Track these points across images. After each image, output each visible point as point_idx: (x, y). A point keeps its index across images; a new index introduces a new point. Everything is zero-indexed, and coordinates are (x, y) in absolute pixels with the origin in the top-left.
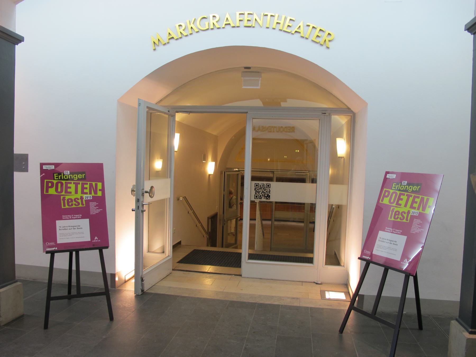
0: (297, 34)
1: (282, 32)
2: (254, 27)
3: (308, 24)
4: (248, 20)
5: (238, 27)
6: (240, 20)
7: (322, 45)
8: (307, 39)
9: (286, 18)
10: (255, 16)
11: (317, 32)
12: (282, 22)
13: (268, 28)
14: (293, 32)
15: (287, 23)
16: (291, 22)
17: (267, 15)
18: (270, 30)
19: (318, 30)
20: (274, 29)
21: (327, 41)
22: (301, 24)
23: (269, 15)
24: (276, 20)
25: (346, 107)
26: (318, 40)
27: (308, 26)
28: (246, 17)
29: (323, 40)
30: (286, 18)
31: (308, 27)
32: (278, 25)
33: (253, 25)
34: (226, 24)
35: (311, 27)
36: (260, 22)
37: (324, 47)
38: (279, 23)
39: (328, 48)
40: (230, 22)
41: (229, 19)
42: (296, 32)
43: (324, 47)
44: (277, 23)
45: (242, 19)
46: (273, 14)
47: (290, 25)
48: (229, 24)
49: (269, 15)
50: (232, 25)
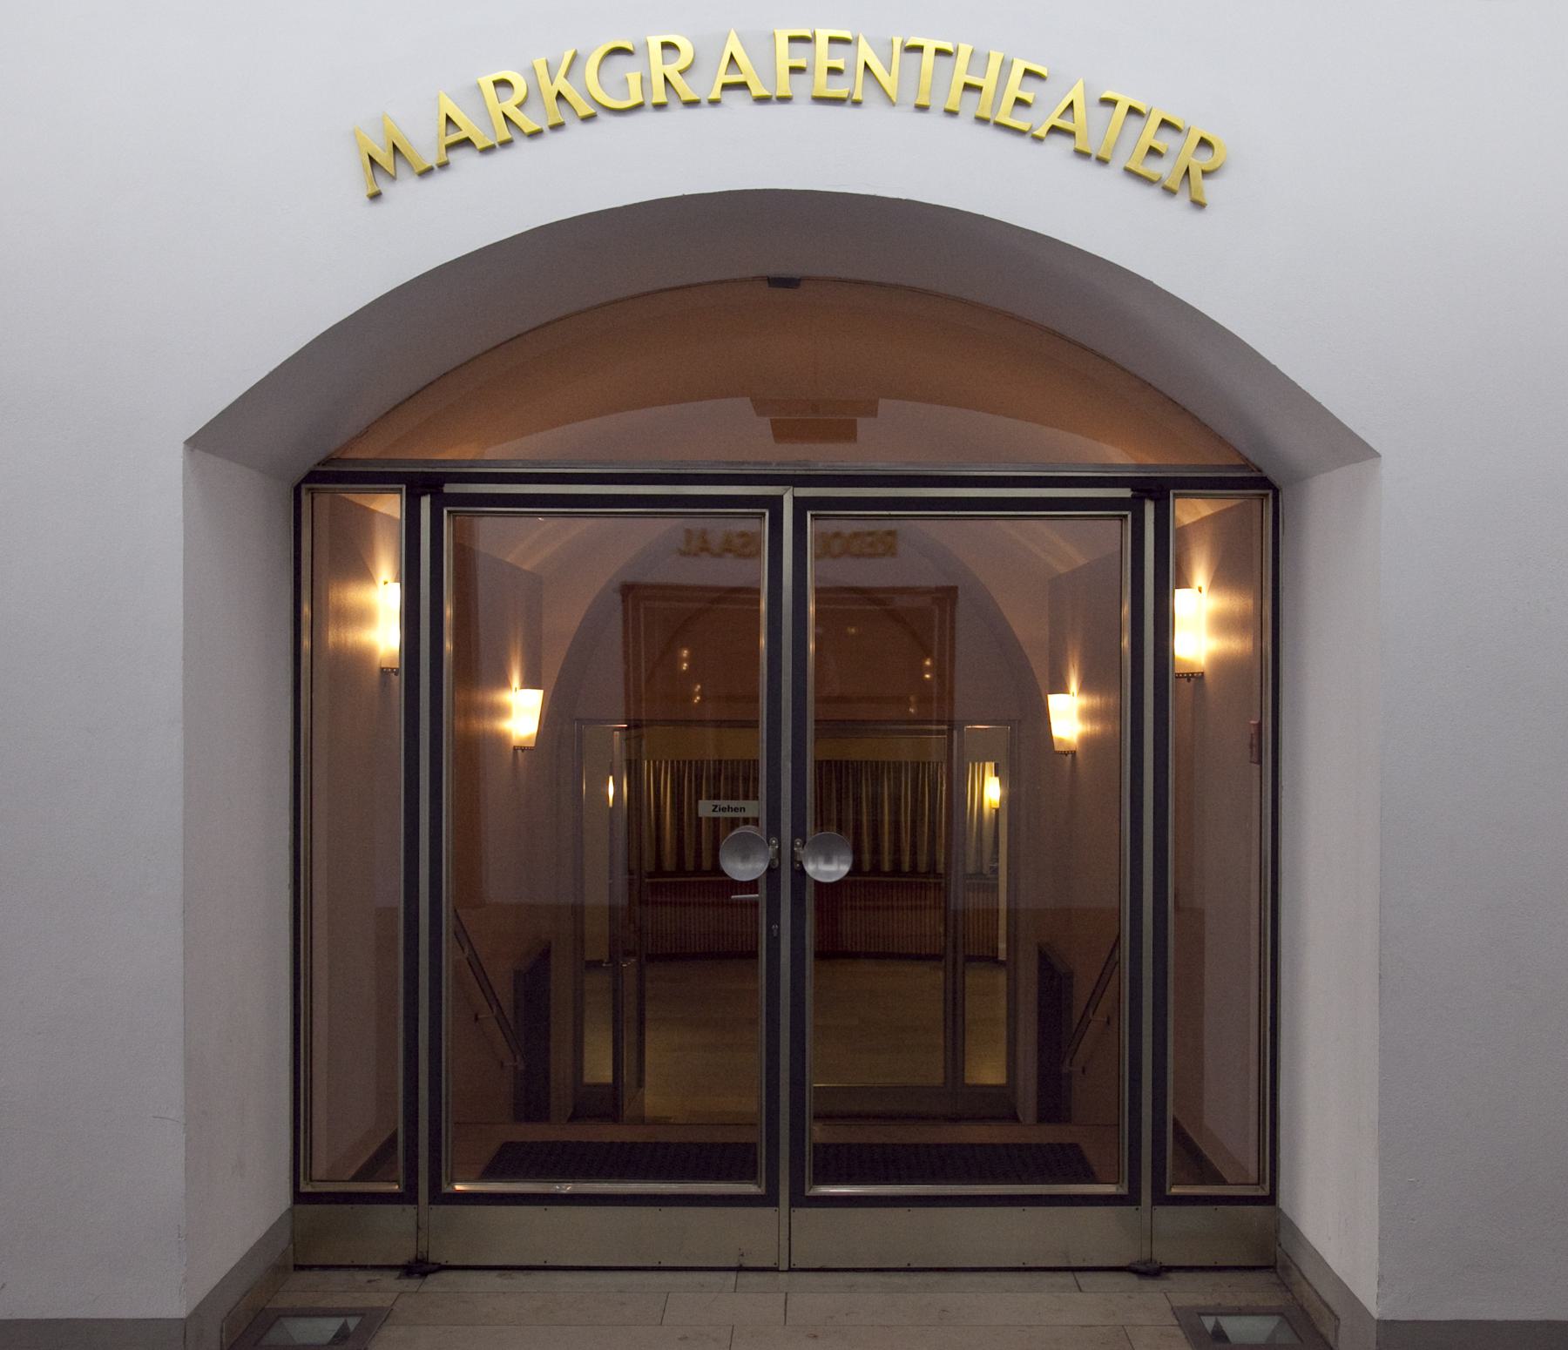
0: (1058, 140)
1: (988, 132)
2: (857, 103)
3: (1108, 95)
4: (832, 71)
5: (784, 100)
6: (794, 70)
7: (1170, 192)
8: (1102, 161)
9: (1006, 66)
10: (865, 53)
11: (1149, 133)
12: (988, 83)
13: (922, 108)
14: (1042, 131)
15: (1014, 88)
16: (1031, 81)
17: (920, 49)
18: (934, 120)
19: (1154, 122)
20: (952, 113)
21: (1195, 173)
22: (1076, 94)
23: (930, 46)
24: (961, 76)
25: (1238, 461)
26: (1154, 168)
27: (1111, 103)
28: (823, 56)
29: (1180, 169)
30: (1006, 66)
31: (1106, 110)
32: (972, 96)
33: (855, 97)
34: (726, 87)
35: (1121, 109)
36: (889, 82)
37: (1182, 201)
38: (979, 89)
39: (1199, 205)
40: (748, 73)
41: (741, 59)
42: (1054, 129)
43: (1182, 201)
44: (968, 87)
45: (801, 63)
46: (949, 47)
47: (1028, 97)
48: (743, 86)
49: (930, 46)
50: (758, 90)
